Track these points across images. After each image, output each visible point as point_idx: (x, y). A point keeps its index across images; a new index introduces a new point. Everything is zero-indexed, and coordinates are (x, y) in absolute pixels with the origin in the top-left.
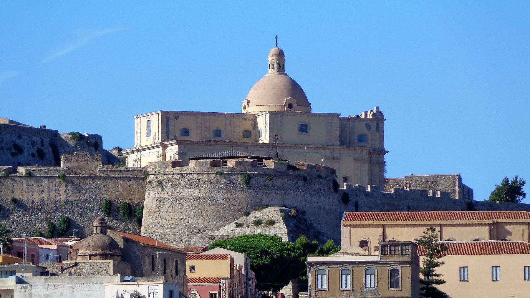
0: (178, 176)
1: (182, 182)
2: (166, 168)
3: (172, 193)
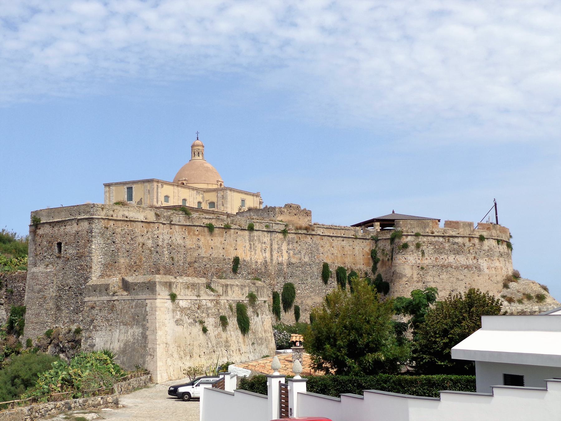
0: (441, 239)
1: (447, 245)
2: (425, 228)
3: (436, 259)
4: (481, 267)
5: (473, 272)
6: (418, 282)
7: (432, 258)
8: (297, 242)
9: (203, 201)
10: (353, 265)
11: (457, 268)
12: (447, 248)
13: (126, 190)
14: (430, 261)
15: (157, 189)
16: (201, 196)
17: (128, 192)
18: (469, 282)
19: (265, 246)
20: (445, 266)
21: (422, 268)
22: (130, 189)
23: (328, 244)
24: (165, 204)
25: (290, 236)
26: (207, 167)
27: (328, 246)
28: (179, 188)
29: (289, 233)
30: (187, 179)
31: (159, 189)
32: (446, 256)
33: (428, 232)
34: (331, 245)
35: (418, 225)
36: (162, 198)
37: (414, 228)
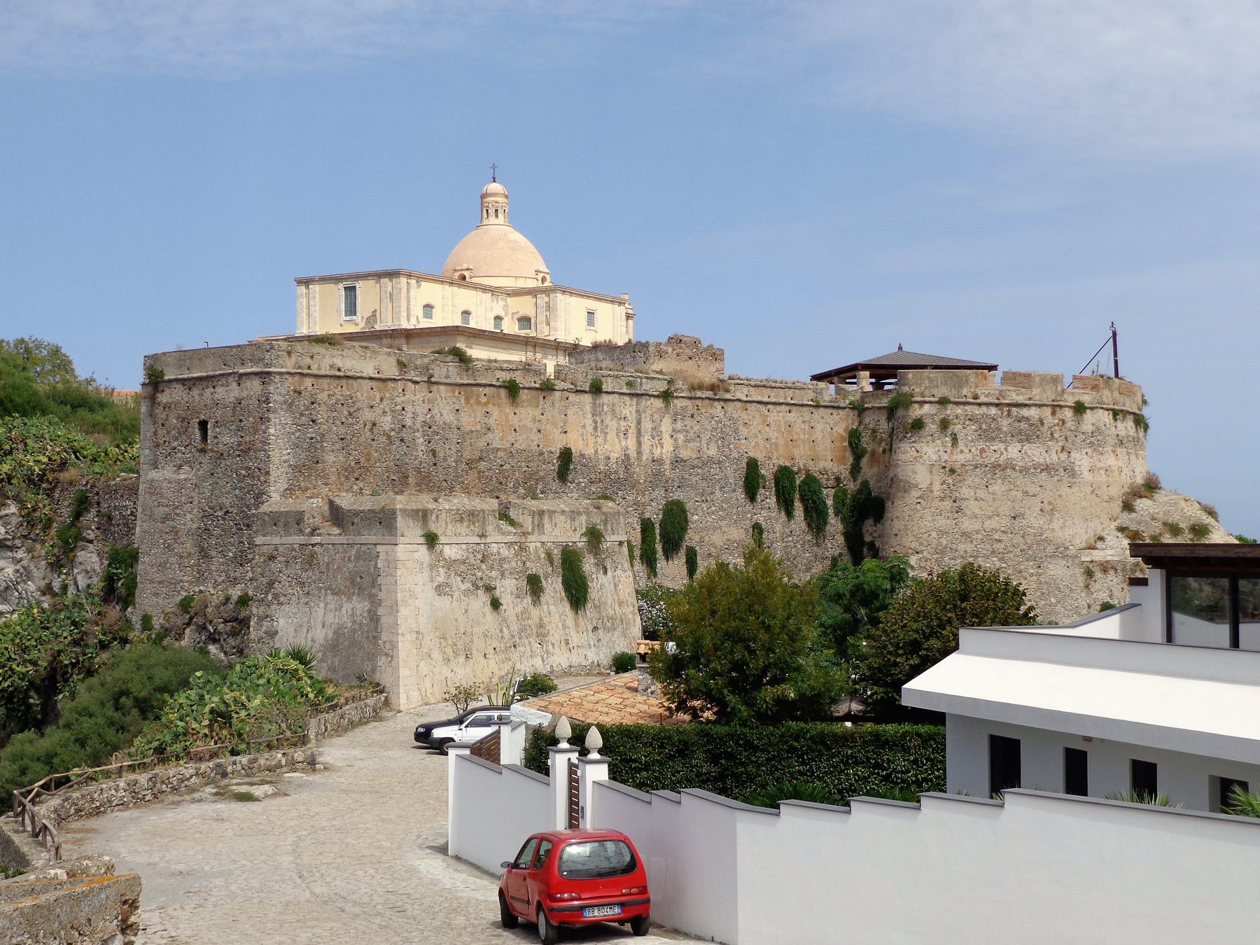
0: (993, 411)
1: (1005, 423)
2: (960, 387)
3: (982, 451)
4: (1077, 468)
5: (1058, 478)
6: (942, 499)
7: (973, 450)
8: (692, 416)
9: (506, 315)
10: (811, 463)
11: (1025, 470)
12: (1005, 429)
13: (343, 292)
14: (969, 456)
15: (408, 290)
16: (502, 303)
17: (346, 296)
18: (1050, 500)
19: (625, 424)
20: (1000, 465)
21: (952, 471)
22: (351, 290)
23: (758, 419)
24: (425, 324)
25: (679, 403)
26: (515, 241)
27: (758, 424)
28: (455, 289)
29: (677, 397)
30: (471, 267)
31: (411, 290)
32: (1002, 446)
33: (965, 396)
34: (764, 421)
35: (946, 382)
36: (418, 311)
37: (937, 386)
